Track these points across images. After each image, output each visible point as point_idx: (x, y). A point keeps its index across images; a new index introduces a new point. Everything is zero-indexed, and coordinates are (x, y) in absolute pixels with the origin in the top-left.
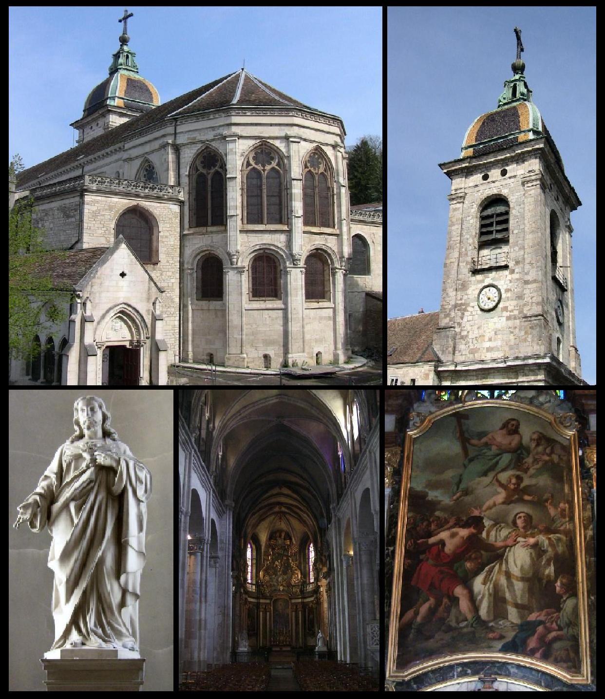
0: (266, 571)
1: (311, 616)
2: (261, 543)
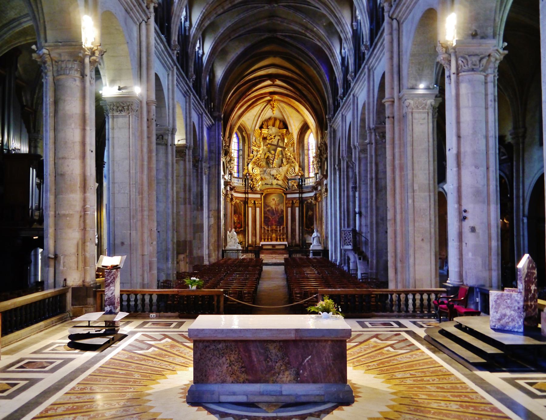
1: (310, 213)
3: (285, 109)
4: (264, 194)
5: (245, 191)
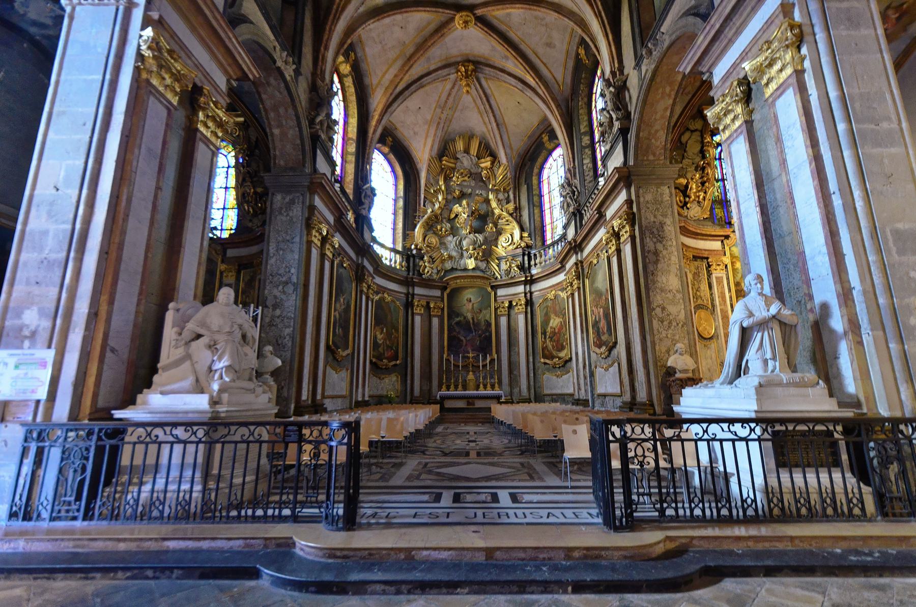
0: (430, 226)
1: (555, 322)
2: (419, 166)
3: (493, 102)
4: (448, 291)
5: (407, 278)
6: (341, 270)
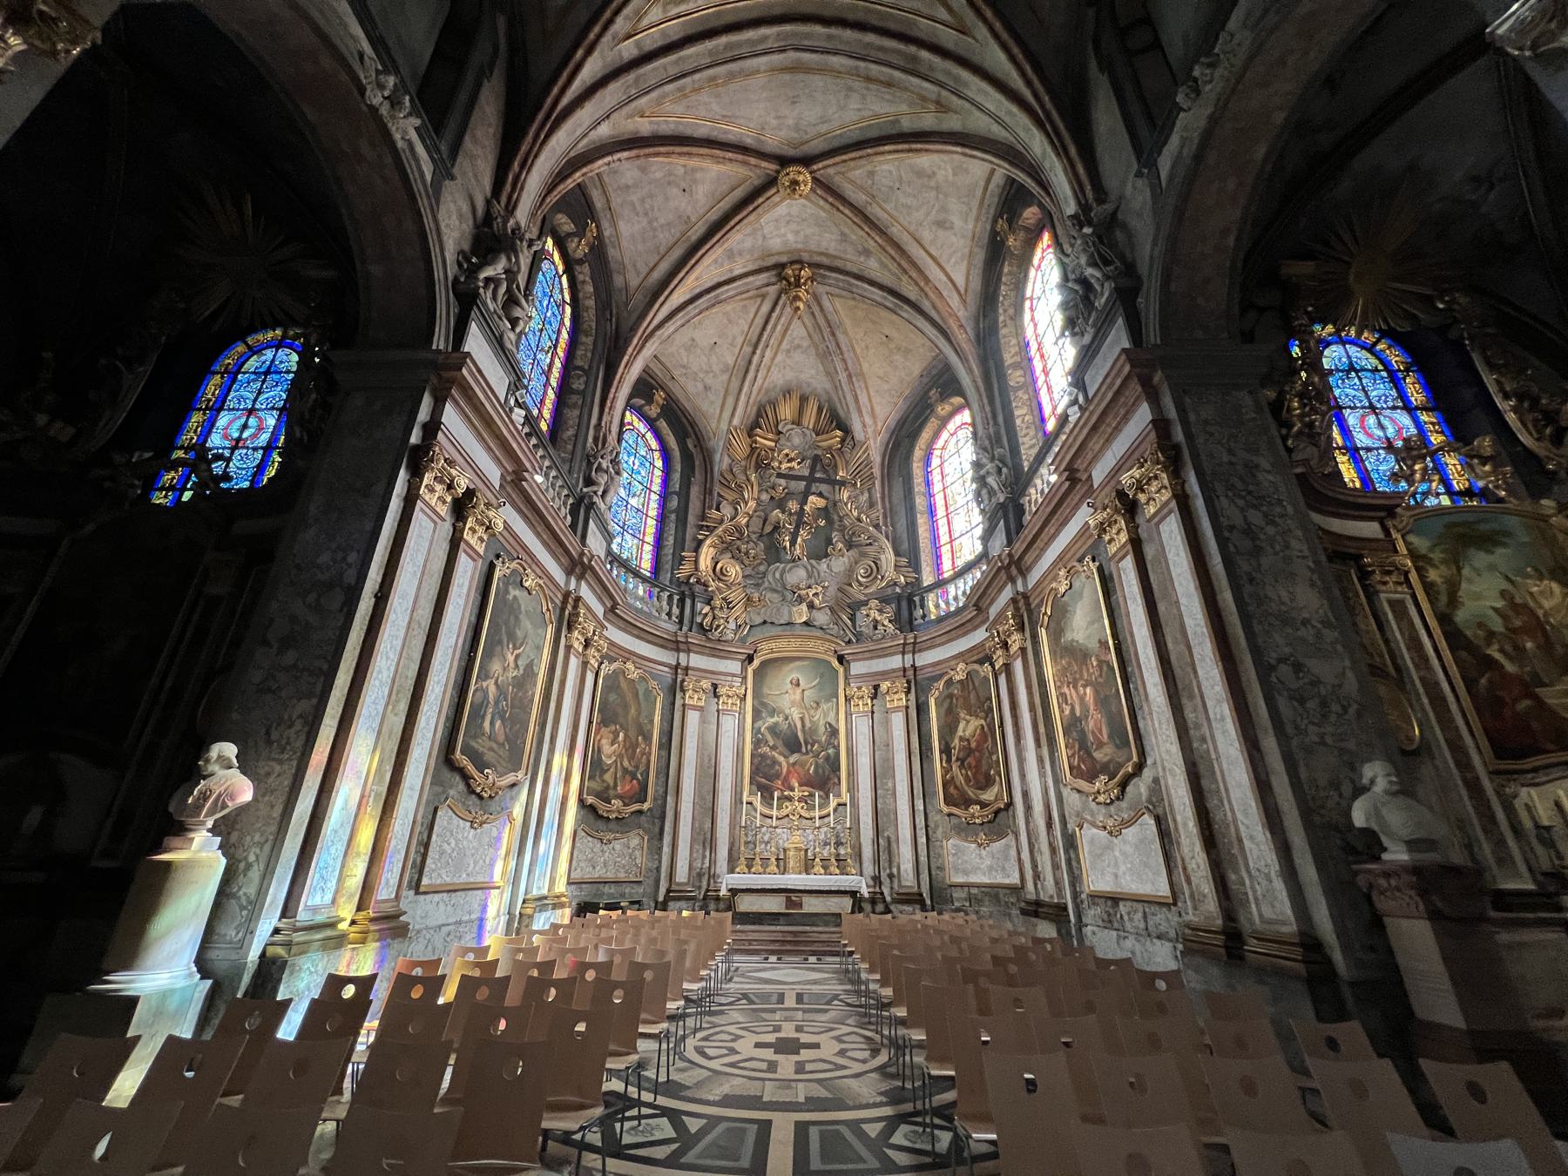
2: (712, 444)
6: (514, 592)
